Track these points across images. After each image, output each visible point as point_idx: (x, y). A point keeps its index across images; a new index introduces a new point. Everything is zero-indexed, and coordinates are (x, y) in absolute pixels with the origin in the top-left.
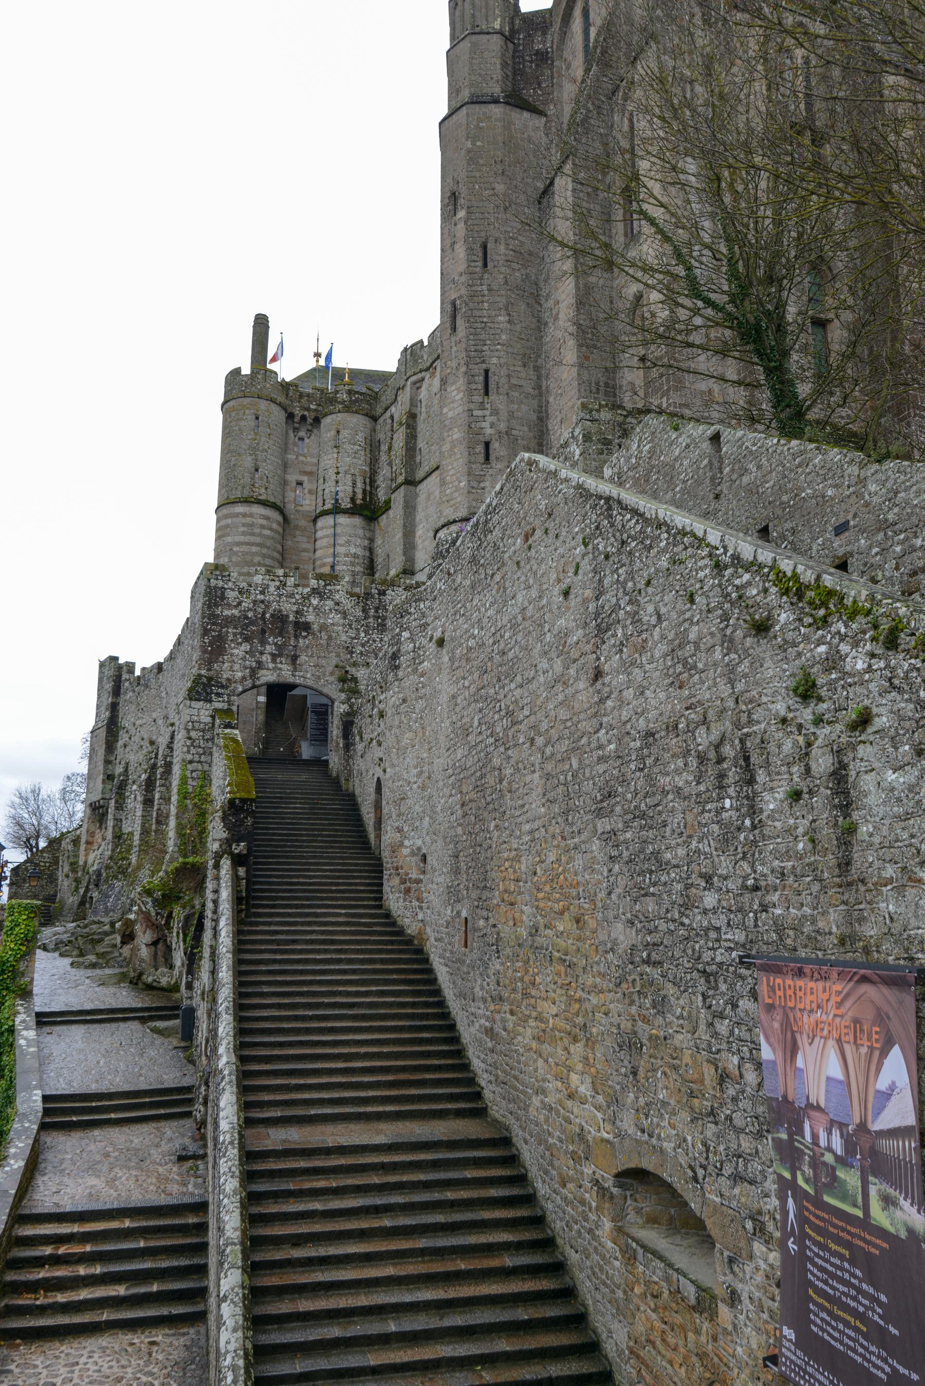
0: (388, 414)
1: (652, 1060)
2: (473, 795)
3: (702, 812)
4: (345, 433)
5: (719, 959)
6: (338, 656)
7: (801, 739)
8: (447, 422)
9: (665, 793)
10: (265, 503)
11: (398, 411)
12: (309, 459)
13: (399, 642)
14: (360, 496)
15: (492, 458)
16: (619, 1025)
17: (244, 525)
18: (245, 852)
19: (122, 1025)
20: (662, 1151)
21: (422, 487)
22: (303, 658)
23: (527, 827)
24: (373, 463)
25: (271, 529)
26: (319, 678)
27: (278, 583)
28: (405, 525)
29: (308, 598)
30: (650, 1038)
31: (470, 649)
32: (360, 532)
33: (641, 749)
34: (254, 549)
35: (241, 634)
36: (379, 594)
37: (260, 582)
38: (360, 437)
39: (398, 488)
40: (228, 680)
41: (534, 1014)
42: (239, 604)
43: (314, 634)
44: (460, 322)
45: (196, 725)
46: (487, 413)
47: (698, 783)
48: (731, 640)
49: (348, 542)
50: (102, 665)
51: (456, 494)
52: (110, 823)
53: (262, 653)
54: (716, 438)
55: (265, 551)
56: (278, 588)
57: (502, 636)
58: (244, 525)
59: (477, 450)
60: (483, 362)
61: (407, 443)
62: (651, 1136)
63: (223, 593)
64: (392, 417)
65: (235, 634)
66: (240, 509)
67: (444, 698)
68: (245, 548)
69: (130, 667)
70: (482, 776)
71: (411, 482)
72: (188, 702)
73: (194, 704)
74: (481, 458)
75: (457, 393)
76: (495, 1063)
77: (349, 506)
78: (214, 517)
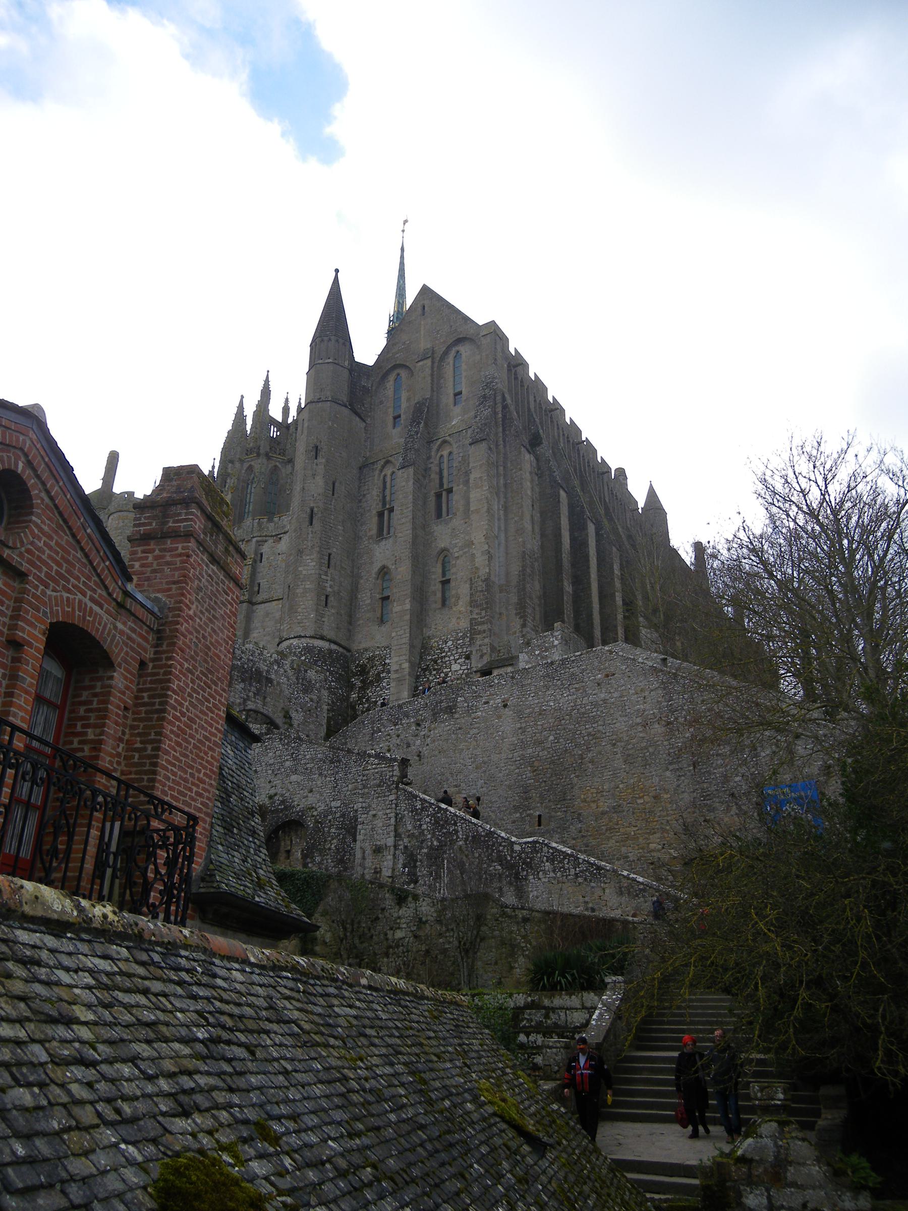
8: (301, 576)
22: (268, 699)
44: (314, 522)
46: (329, 578)
51: (305, 621)
53: (249, 691)
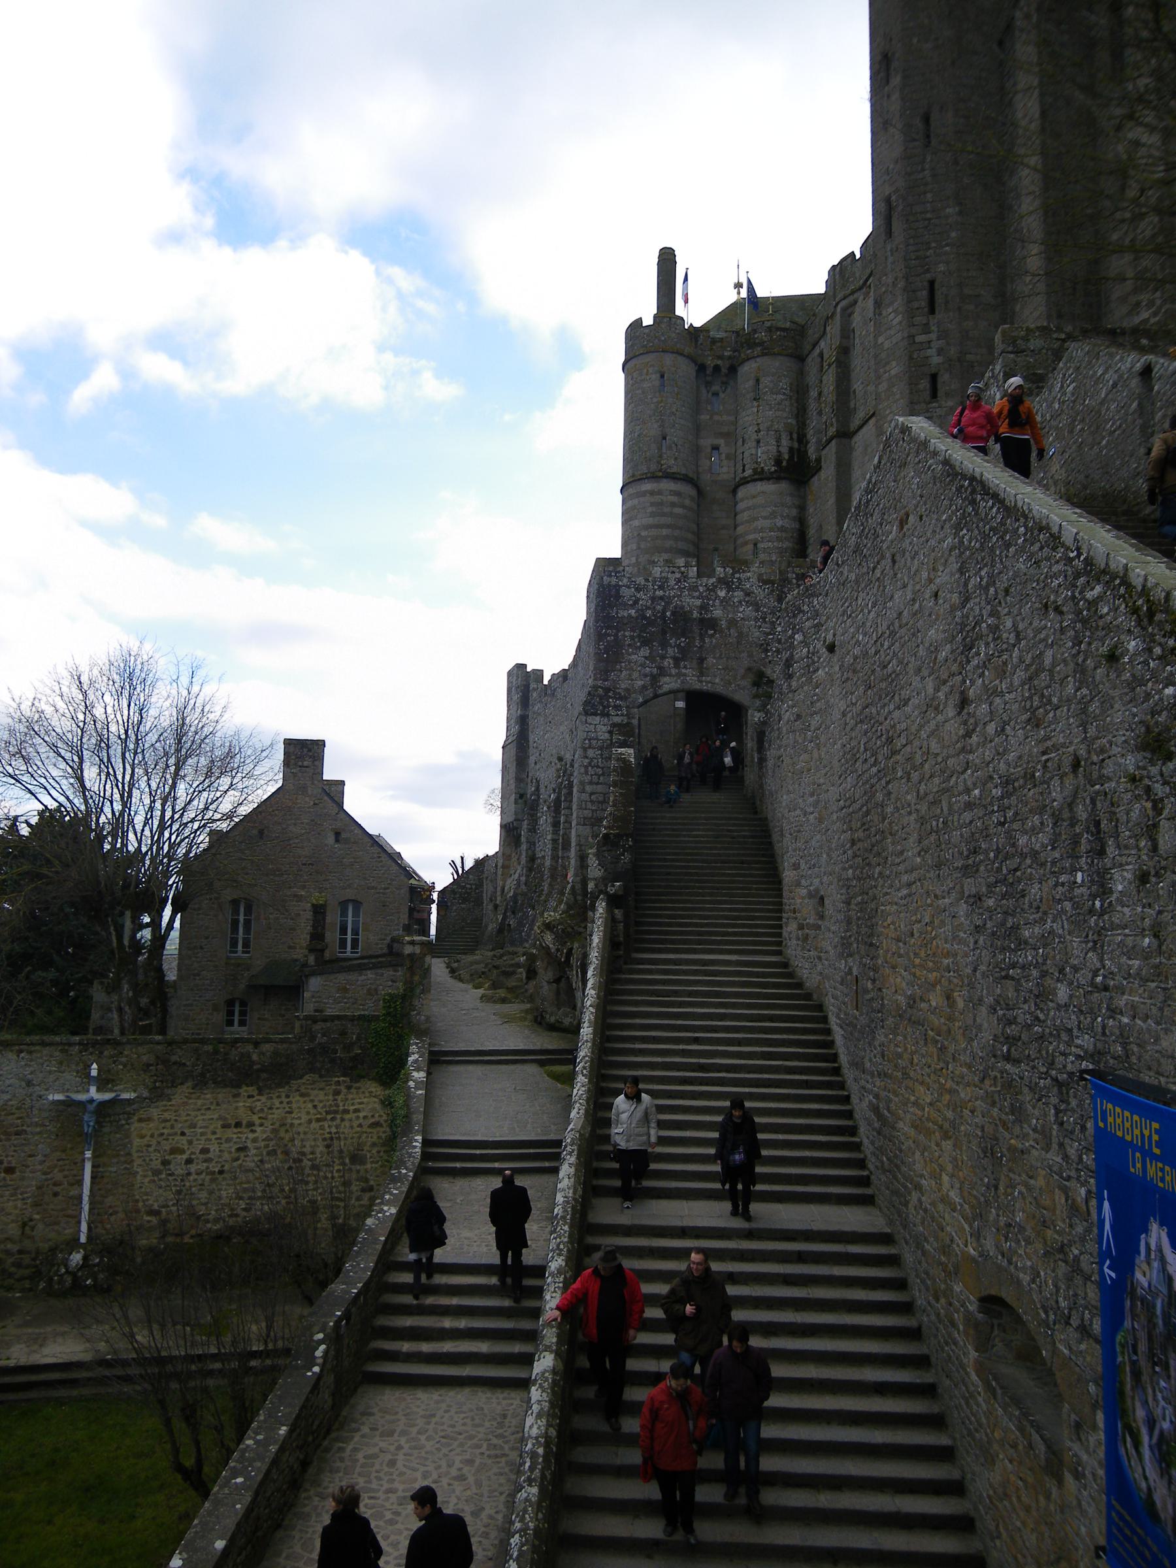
0: (817, 351)
1: (1011, 1175)
2: (860, 834)
3: (1056, 885)
4: (766, 381)
5: (1069, 1067)
6: (750, 655)
7: (1149, 805)
9: (1023, 856)
10: (673, 477)
11: (828, 346)
12: (725, 417)
13: (792, 647)
14: (786, 457)
15: (940, 393)
16: (983, 1127)
17: (652, 504)
18: (621, 893)
19: (519, 1067)
20: (1019, 1282)
21: (859, 438)
22: (711, 660)
23: (905, 878)
24: (801, 413)
25: (683, 506)
26: (730, 683)
27: (678, 575)
28: (838, 488)
29: (713, 590)
30: (1009, 1149)
31: (856, 658)
32: (788, 500)
33: (1002, 798)
34: (665, 532)
35: (639, 636)
36: (798, 579)
37: (658, 575)
38: (784, 383)
39: (829, 441)
40: (627, 690)
41: (913, 1098)
42: (636, 602)
43: (721, 631)
44: (897, 226)
45: (594, 742)
46: (933, 336)
47: (1054, 848)
48: (1083, 672)
49: (773, 515)
50: (510, 674)
52: (524, 847)
53: (663, 657)
54: (1147, 371)
55: (677, 533)
56: (679, 581)
57: (882, 645)
58: (652, 504)
59: (921, 387)
60: (928, 271)
61: (838, 386)
62: (1010, 1262)
63: (618, 592)
64: (821, 355)
65: (632, 638)
66: (647, 486)
67: (836, 715)
68: (654, 532)
69: (539, 674)
70: (868, 813)
71: (845, 434)
72: (584, 718)
73: (590, 719)
74: (927, 395)
75: (894, 316)
76: (881, 1147)
77: (773, 469)
78: (620, 497)
